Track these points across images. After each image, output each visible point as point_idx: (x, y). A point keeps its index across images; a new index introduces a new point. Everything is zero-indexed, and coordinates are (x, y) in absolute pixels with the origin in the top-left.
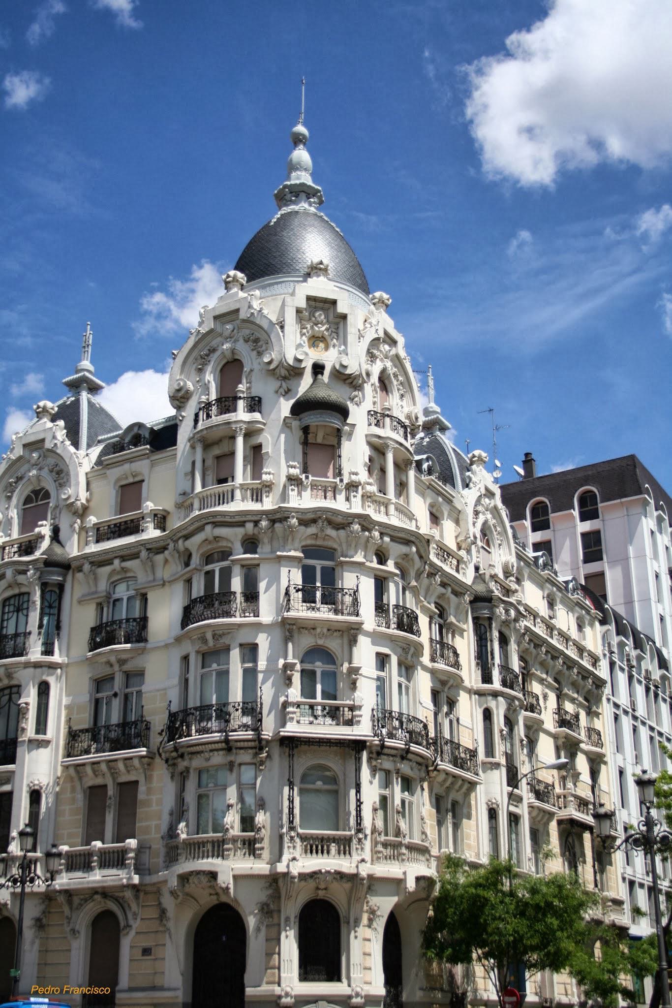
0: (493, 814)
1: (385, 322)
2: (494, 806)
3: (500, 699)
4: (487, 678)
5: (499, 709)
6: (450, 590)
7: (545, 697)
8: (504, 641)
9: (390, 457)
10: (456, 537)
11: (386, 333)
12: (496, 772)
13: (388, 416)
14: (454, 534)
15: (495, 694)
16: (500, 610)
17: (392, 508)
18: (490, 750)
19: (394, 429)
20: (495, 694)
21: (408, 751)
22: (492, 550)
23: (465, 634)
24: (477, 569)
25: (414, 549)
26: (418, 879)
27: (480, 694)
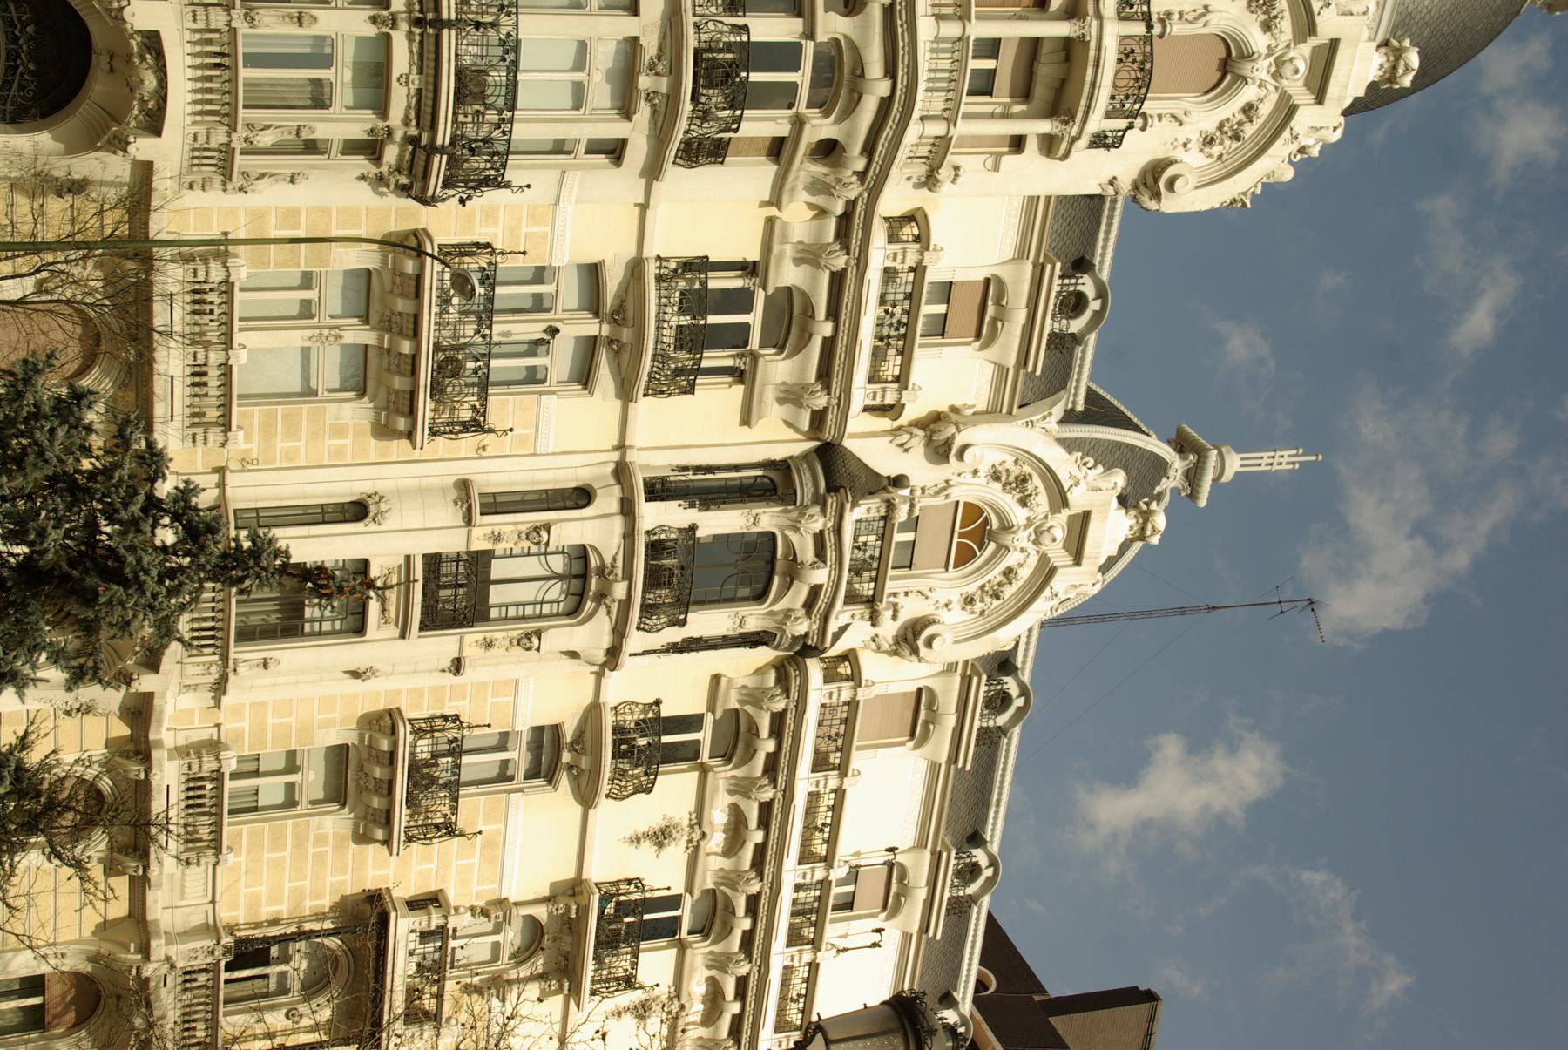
0: (358, 511)
1: (1358, 69)
2: (373, 509)
3: (618, 524)
4: (659, 490)
5: (595, 529)
6: (827, 329)
7: (661, 837)
8: (757, 568)
9: (1063, 29)
10: (954, 409)
11: (1334, 44)
12: (453, 516)
13: (1150, 27)
14: (957, 403)
15: (627, 509)
16: (818, 522)
17: (952, 29)
18: (496, 505)
19: (1125, 55)
20: (627, 509)
21: (440, 24)
22: (953, 573)
23: (746, 434)
24: (898, 481)
25: (883, 88)
26: (153, 42)
27: (621, 472)
